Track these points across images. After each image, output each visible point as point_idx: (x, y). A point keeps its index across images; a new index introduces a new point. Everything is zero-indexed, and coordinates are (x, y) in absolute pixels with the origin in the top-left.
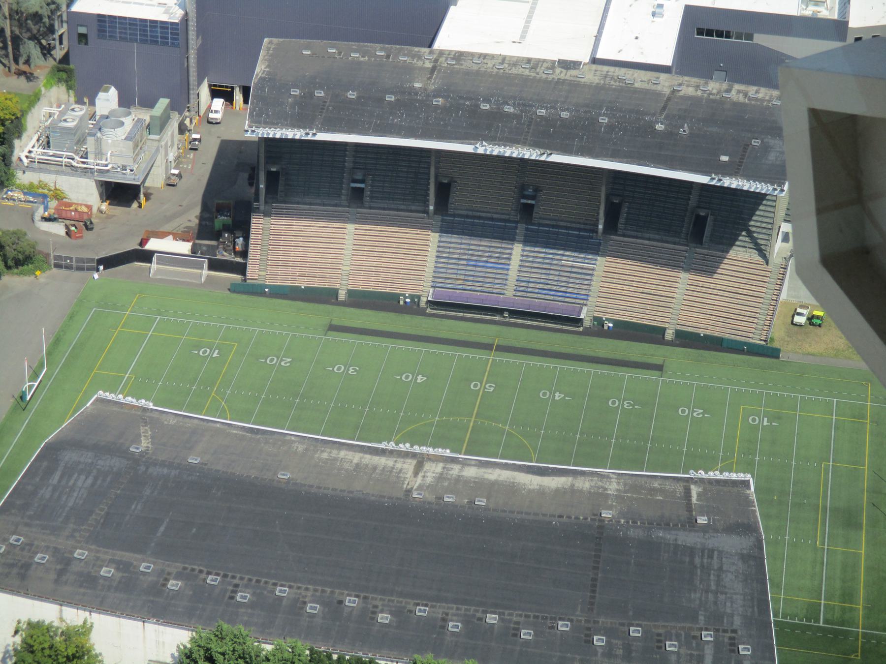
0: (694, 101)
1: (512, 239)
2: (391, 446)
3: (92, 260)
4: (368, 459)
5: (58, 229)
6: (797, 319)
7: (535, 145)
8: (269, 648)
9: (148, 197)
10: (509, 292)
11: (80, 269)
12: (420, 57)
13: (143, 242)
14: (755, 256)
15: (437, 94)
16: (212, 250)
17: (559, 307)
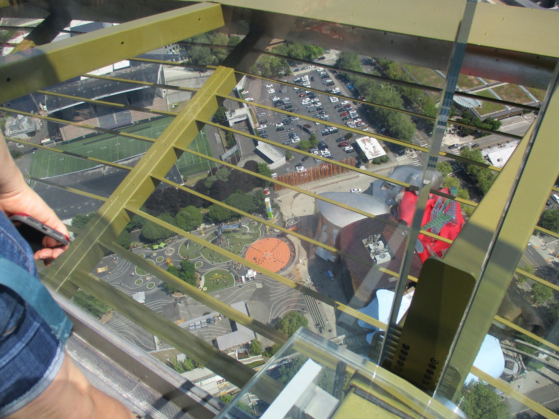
0: (135, 72)
1: (112, 113)
2: (98, 166)
3: (31, 150)
4: (94, 171)
5: (22, 146)
6: (173, 107)
7: (106, 94)
8: (88, 215)
9: (38, 132)
10: (116, 123)
11: (30, 153)
12: (78, 83)
13: (41, 142)
14: (159, 98)
15: (83, 90)
16: (54, 138)
17: (127, 122)
